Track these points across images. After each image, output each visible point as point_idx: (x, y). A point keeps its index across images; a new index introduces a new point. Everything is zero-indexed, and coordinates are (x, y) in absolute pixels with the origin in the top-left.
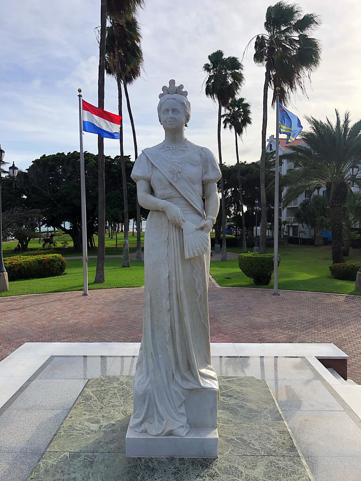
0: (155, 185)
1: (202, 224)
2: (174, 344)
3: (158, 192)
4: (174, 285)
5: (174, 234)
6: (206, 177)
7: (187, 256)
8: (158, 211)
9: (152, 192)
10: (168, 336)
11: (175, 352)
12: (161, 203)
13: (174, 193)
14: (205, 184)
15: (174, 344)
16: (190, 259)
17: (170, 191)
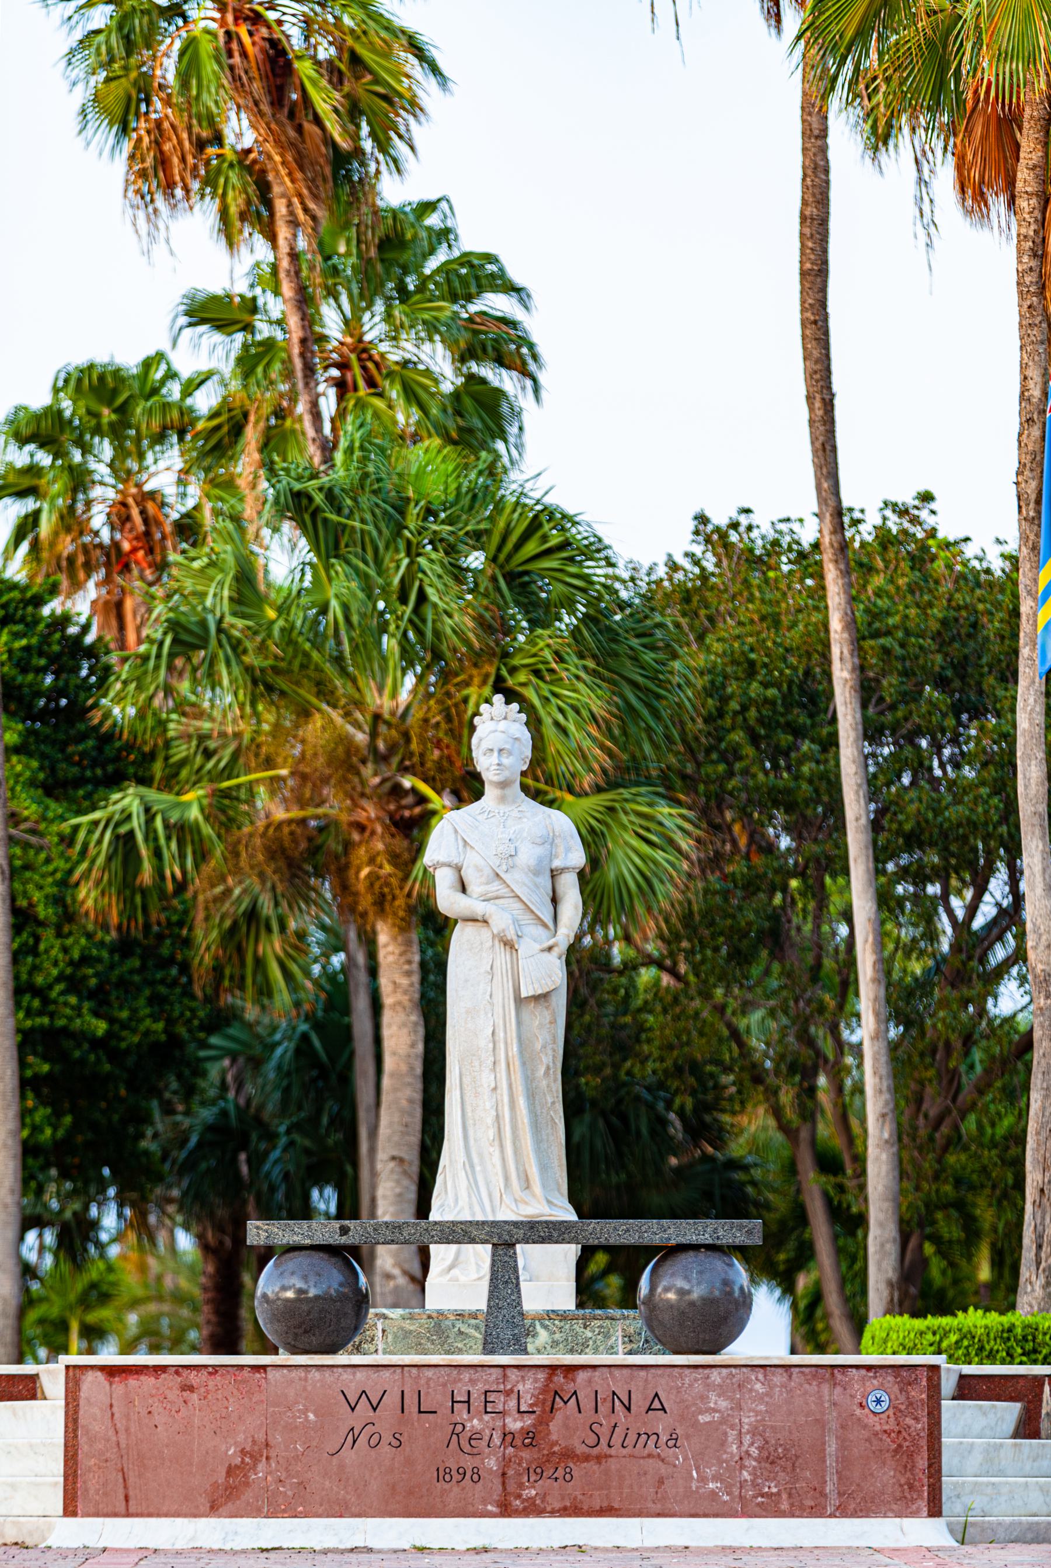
0: (469, 875)
1: (551, 942)
2: (501, 1146)
3: (473, 888)
4: (502, 1046)
5: (502, 957)
6: (557, 863)
7: (524, 994)
8: (475, 920)
9: (464, 890)
10: (491, 1133)
11: (504, 1160)
12: (479, 908)
13: (504, 891)
14: (554, 874)
15: (501, 1146)
16: (529, 999)
17: (496, 887)
